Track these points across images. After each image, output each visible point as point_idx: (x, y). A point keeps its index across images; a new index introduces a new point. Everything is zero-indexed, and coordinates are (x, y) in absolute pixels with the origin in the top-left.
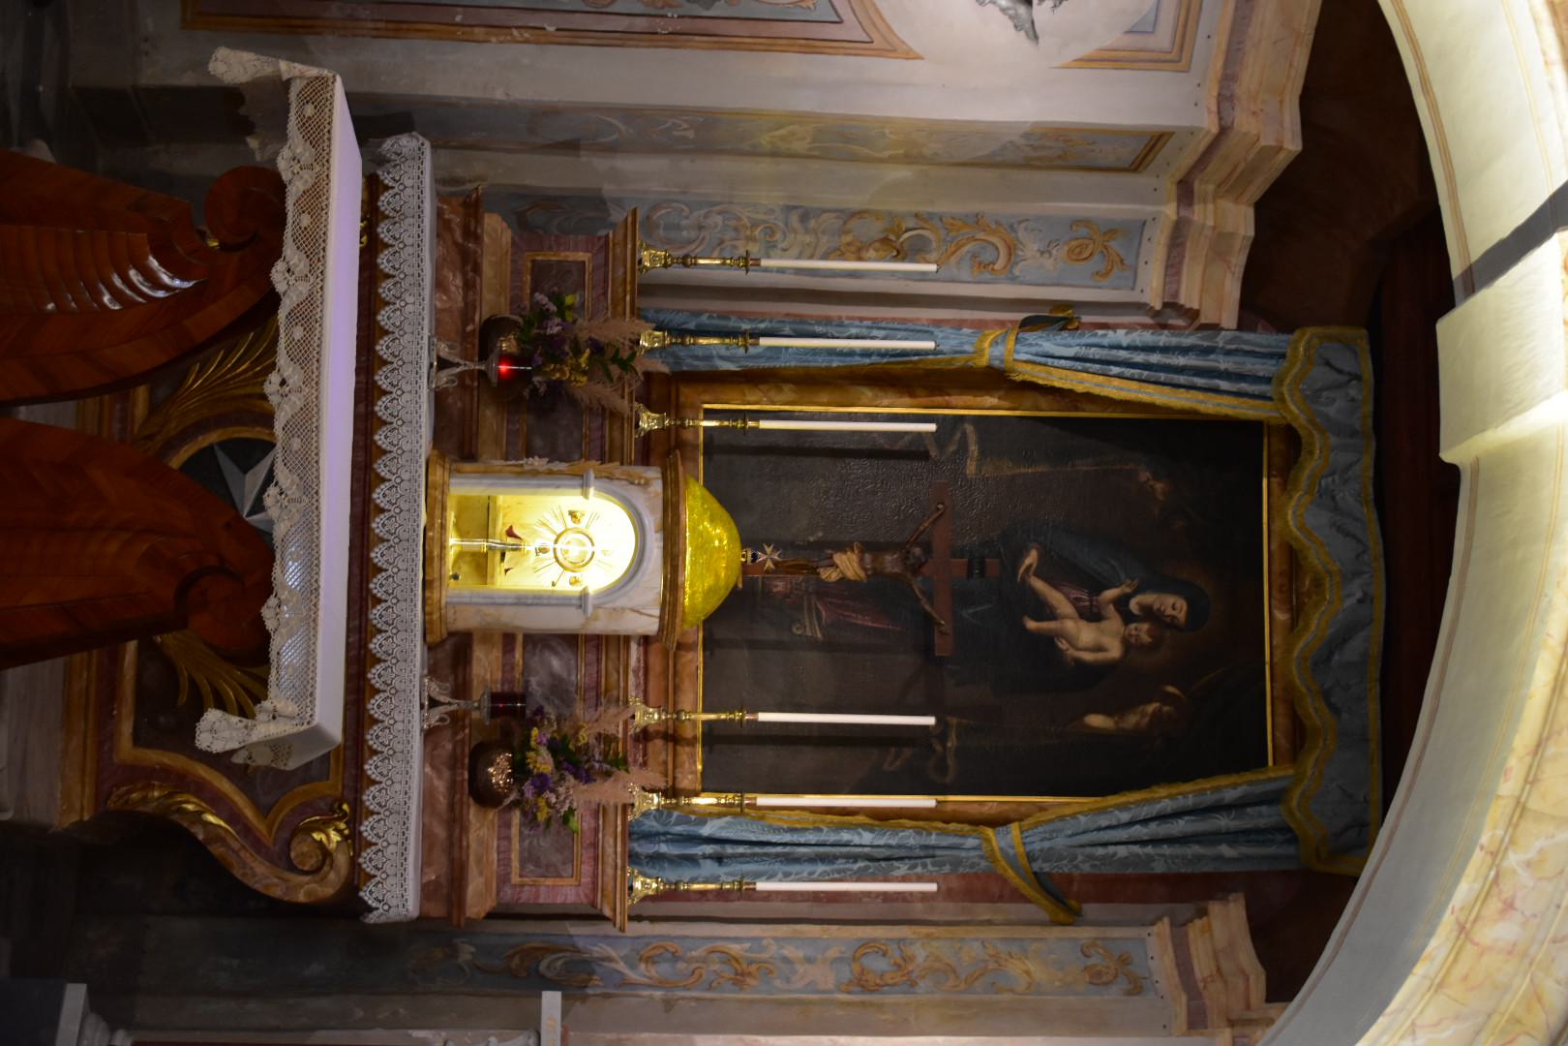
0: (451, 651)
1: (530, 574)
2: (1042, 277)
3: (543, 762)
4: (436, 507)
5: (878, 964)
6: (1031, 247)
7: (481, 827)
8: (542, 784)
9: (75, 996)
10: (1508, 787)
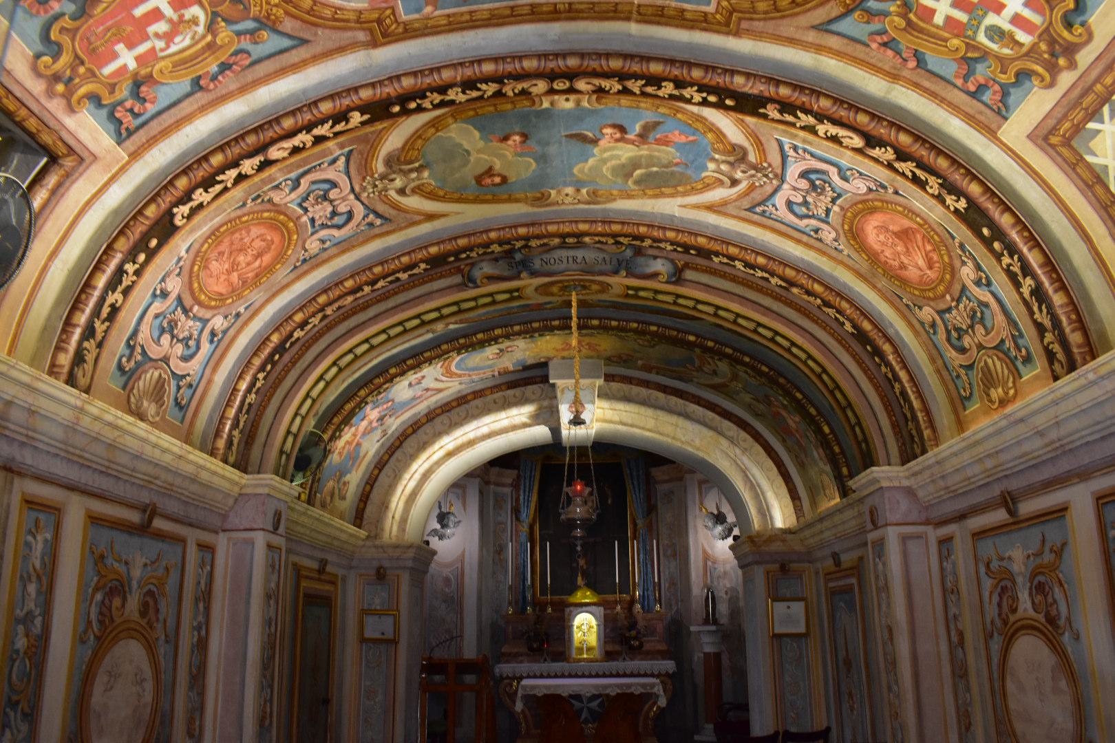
0: (609, 655)
1: (593, 639)
2: (507, 516)
3: (633, 633)
4: (580, 661)
5: (669, 552)
6: (500, 519)
7: (647, 647)
8: (639, 632)
9: (696, 738)
10: (669, 440)
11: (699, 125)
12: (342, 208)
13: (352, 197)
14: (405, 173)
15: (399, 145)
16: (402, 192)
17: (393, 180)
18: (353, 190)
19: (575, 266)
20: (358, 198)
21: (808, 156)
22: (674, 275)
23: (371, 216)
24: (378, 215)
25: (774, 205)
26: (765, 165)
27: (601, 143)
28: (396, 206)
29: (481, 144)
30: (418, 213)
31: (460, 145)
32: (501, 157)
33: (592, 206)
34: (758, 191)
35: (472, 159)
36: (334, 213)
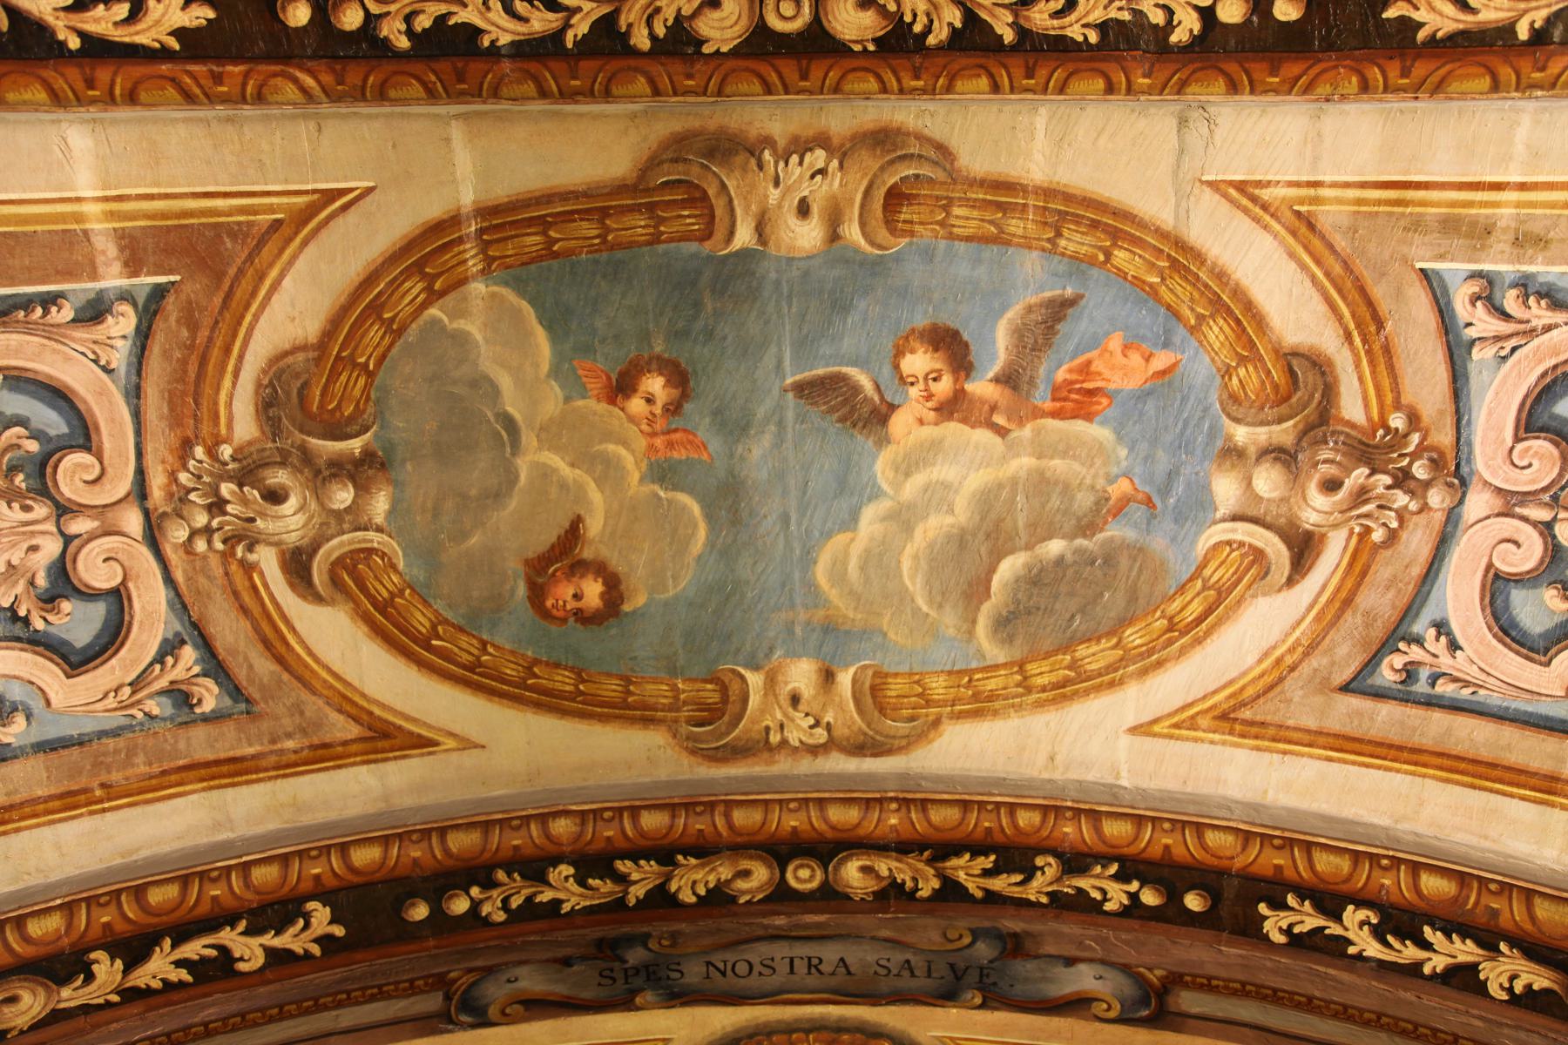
11: (1178, 292)
12: (94, 571)
13: (133, 521)
14: (322, 474)
15: (310, 328)
16: (297, 565)
17: (275, 497)
18: (141, 490)
19: (813, 981)
20: (153, 538)
21: (1539, 314)
22: (1144, 1001)
23: (189, 654)
24: (215, 666)
25: (1441, 627)
26: (1397, 421)
27: (900, 423)
28: (274, 639)
29: (552, 400)
30: (347, 702)
31: (496, 392)
32: (607, 471)
33: (870, 765)
34: (1382, 571)
35: (523, 465)
36: (63, 583)
